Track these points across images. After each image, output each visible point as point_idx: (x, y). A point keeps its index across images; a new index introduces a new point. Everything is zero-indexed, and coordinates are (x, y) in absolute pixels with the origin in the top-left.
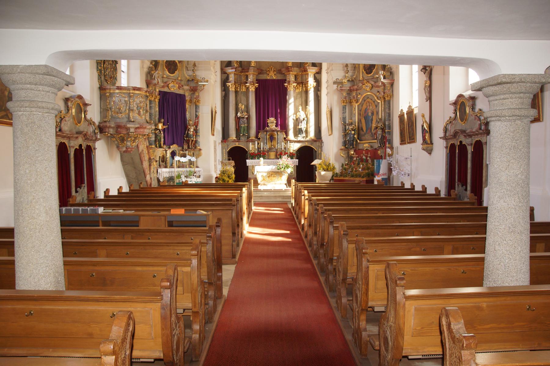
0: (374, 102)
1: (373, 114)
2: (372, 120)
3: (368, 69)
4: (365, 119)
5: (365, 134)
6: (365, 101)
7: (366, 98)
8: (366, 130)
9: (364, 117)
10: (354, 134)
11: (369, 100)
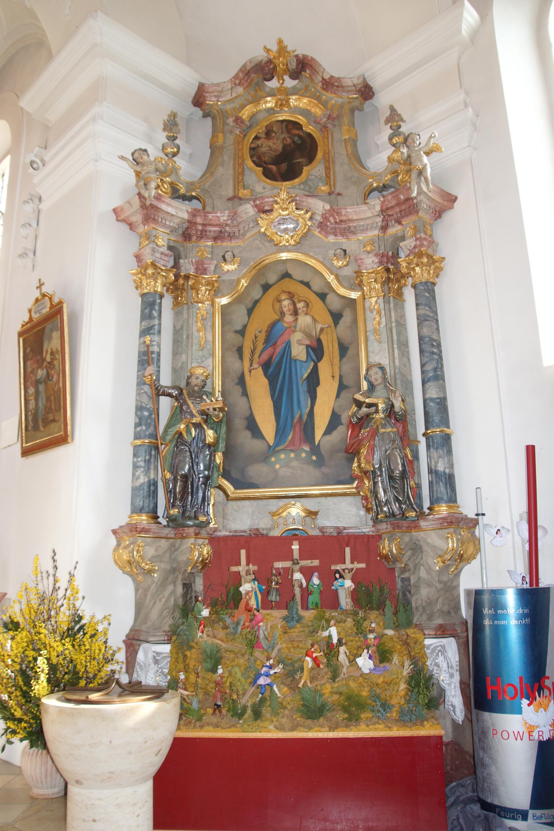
0: (322, 296)
1: (316, 350)
2: (313, 381)
3: (278, 160)
4: (272, 380)
5: (272, 450)
6: (266, 287)
7: (272, 278)
8: (280, 433)
9: (266, 366)
10: (213, 447)
11: (287, 284)
